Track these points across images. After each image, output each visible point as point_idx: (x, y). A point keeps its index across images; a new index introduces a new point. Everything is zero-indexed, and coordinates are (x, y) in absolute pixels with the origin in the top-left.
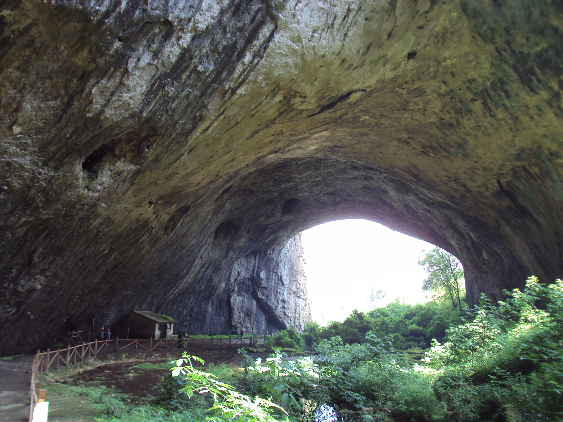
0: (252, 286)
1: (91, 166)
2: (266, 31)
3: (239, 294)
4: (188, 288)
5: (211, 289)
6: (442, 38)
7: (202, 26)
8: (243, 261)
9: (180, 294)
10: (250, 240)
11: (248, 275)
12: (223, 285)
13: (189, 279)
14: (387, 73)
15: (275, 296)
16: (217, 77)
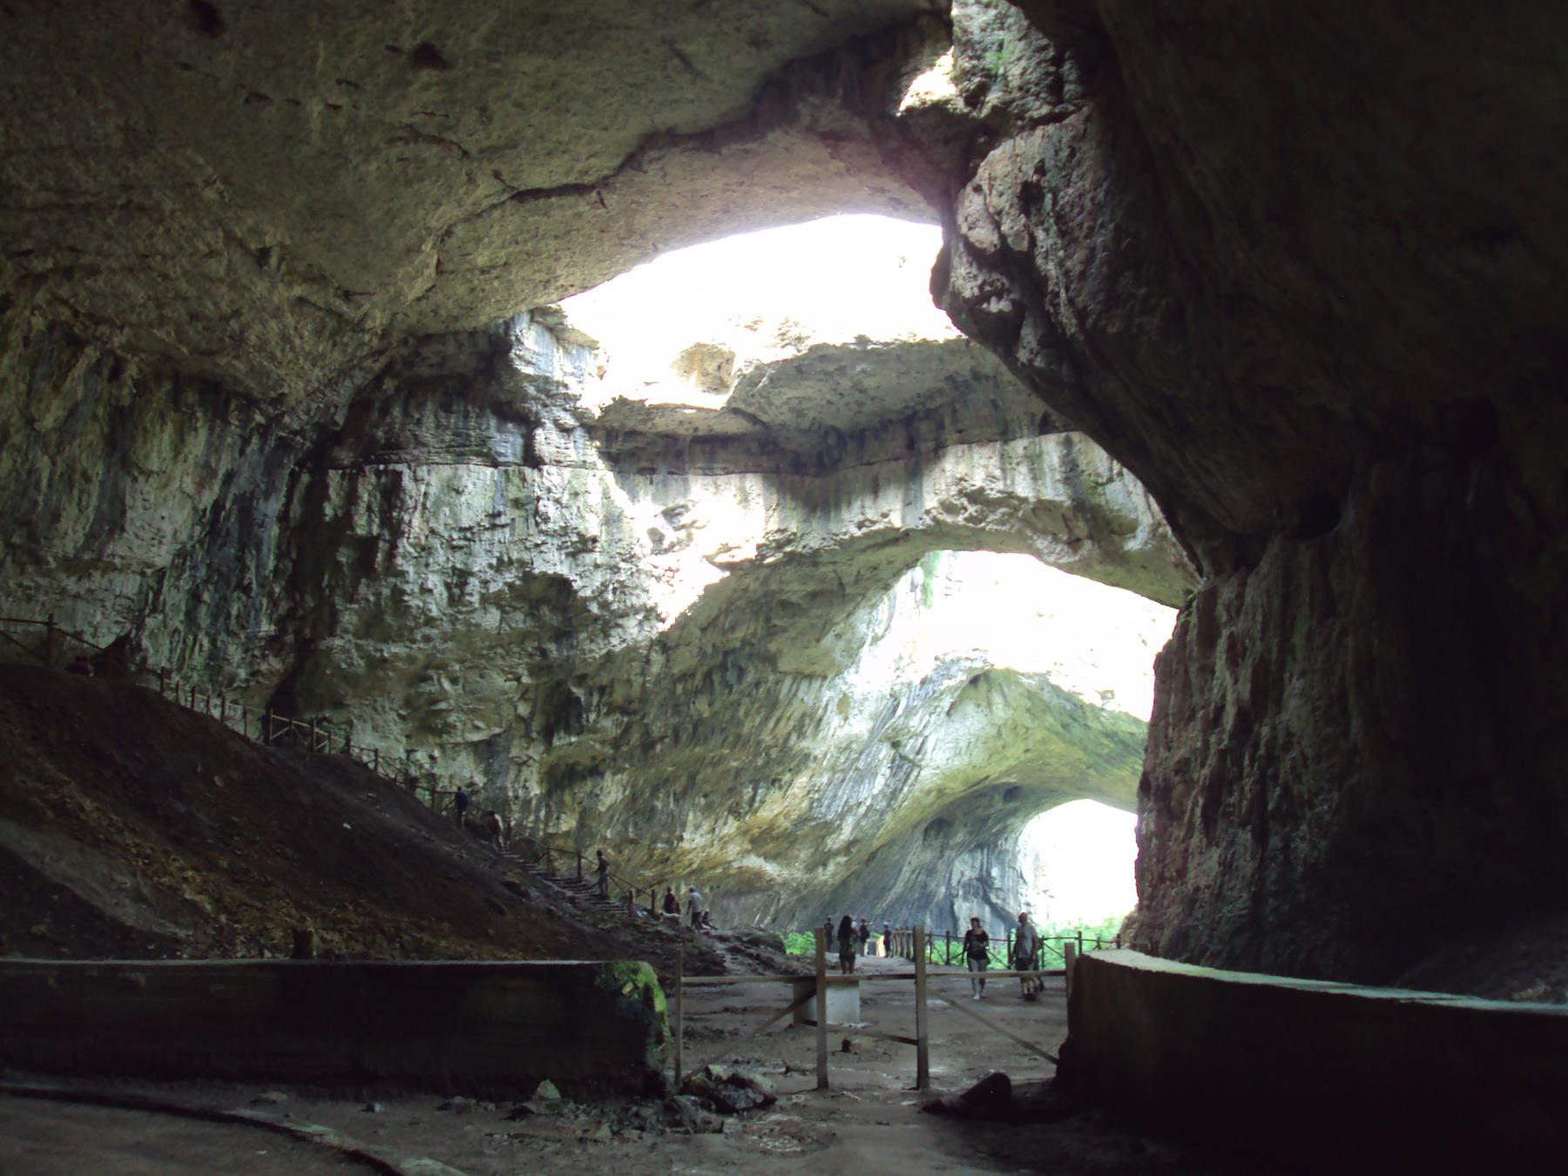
0: (983, 886)
1: (825, 865)
2: (915, 773)
3: (965, 899)
4: (898, 899)
5: (926, 898)
6: (1044, 742)
7: (875, 791)
8: (966, 857)
9: (891, 906)
10: (971, 833)
11: (975, 874)
12: (943, 889)
13: (898, 888)
14: (1012, 762)
15: (1016, 898)
16: (889, 805)
